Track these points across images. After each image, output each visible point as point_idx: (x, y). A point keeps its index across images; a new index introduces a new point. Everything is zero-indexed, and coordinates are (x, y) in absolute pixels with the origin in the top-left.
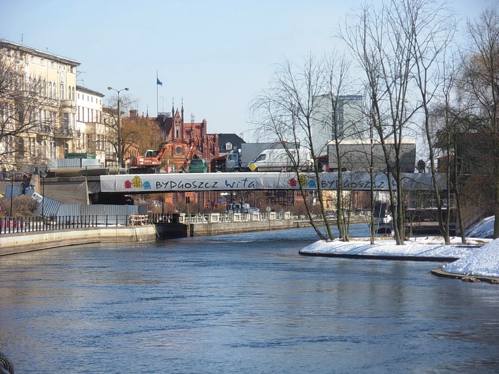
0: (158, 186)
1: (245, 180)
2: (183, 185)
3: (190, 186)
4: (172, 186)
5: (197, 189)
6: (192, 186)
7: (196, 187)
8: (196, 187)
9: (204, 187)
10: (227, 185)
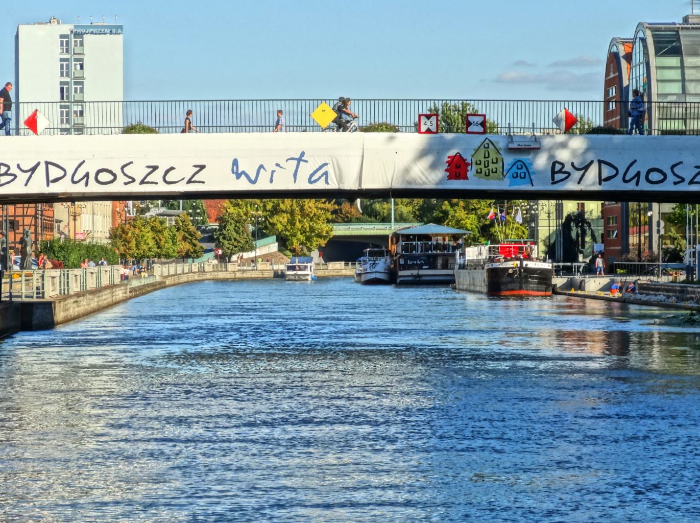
2: (87, 175)
3: (112, 178)
4: (51, 178)
5: (135, 188)
6: (121, 179)
7: (134, 180)
8: (134, 180)
9: (160, 181)
10: (238, 176)
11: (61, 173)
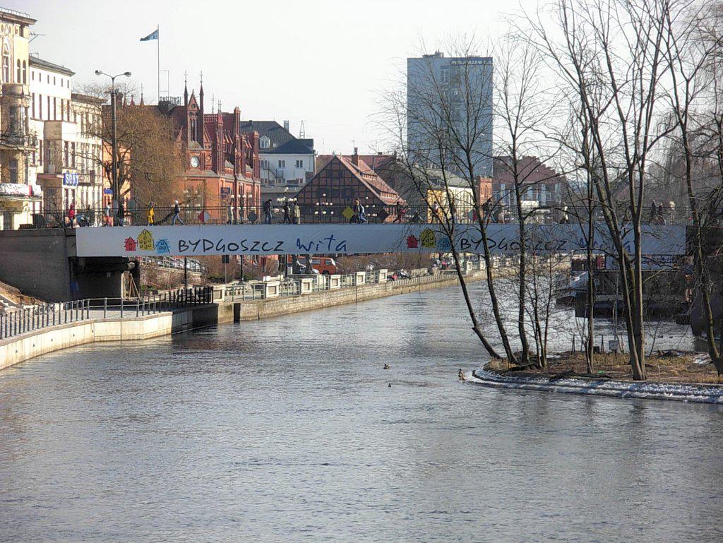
0: (182, 248)
1: (331, 239)
2: (224, 246)
3: (236, 248)
6: (241, 248)
7: (247, 249)
8: (247, 249)
11: (211, 245)
